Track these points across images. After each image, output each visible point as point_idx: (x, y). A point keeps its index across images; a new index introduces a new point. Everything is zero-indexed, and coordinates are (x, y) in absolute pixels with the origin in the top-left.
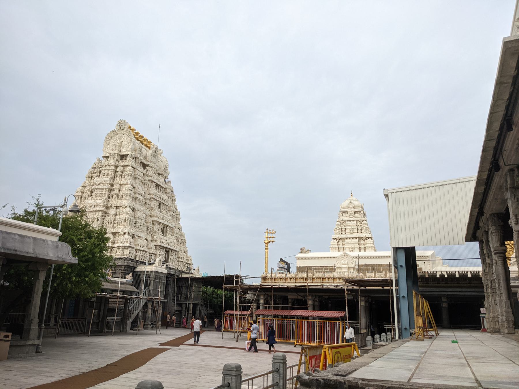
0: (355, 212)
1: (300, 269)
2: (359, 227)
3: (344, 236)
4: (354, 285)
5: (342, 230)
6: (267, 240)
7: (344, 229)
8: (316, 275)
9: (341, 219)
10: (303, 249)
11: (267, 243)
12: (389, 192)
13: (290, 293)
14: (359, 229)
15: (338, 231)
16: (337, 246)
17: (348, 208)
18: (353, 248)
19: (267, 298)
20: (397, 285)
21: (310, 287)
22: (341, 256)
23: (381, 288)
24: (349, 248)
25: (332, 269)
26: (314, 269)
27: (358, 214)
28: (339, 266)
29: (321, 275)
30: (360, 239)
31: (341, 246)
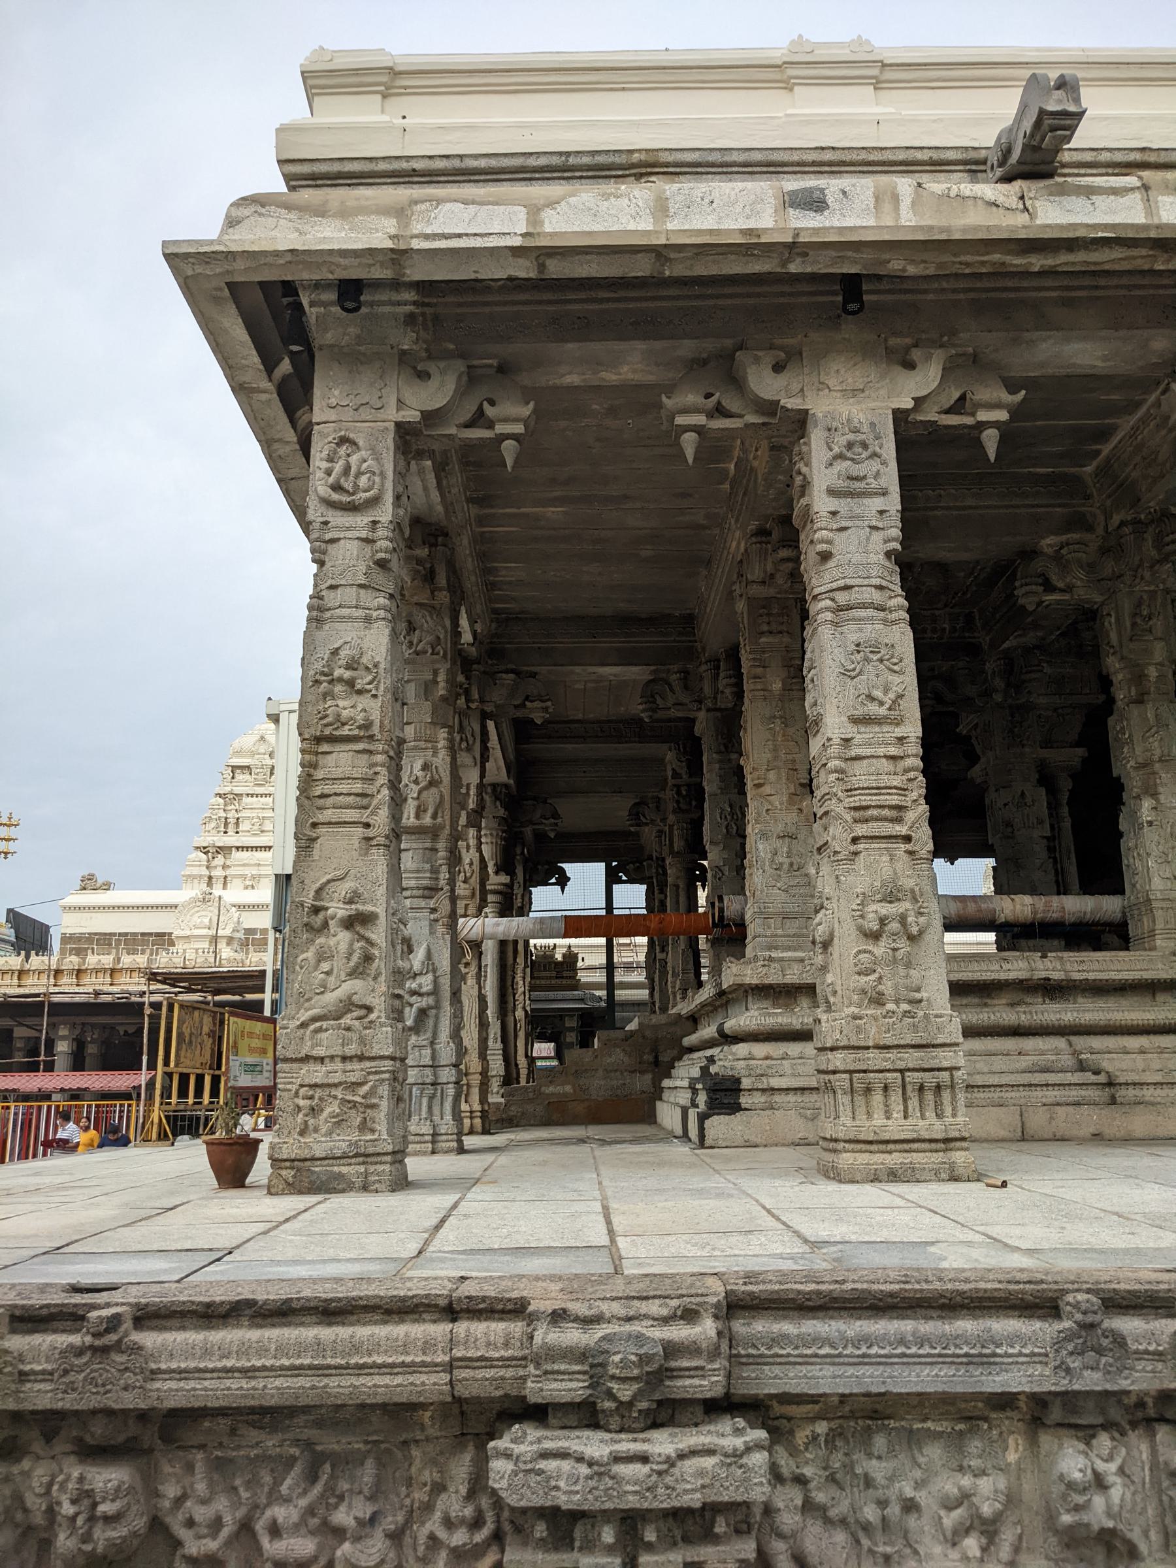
1: (78, 943)
3: (230, 840)
4: (190, 990)
5: (226, 824)
7: (232, 821)
8: (92, 960)
9: (227, 789)
12: (282, 707)
13: (61, 1018)
15: (213, 825)
17: (252, 754)
18: (253, 877)
20: (275, 989)
21: (56, 999)
22: (195, 900)
23: (237, 998)
24: (244, 877)
25: (163, 940)
26: (118, 942)
28: (182, 933)
29: (107, 960)
31: (218, 872)
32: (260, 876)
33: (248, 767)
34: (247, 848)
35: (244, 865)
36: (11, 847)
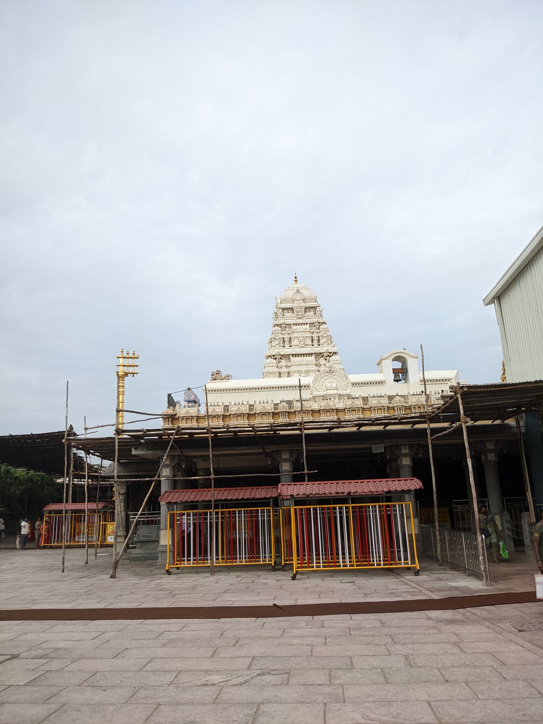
0: (306, 308)
2: (315, 335)
3: (287, 351)
5: (284, 342)
6: (121, 370)
9: (281, 322)
10: (218, 373)
11: (121, 377)
14: (316, 338)
15: (277, 342)
16: (277, 370)
19: (179, 464)
27: (312, 313)
30: (319, 355)
31: (284, 370)
32: (309, 371)
33: (292, 309)
34: (298, 355)
35: (299, 365)
36: (135, 370)
